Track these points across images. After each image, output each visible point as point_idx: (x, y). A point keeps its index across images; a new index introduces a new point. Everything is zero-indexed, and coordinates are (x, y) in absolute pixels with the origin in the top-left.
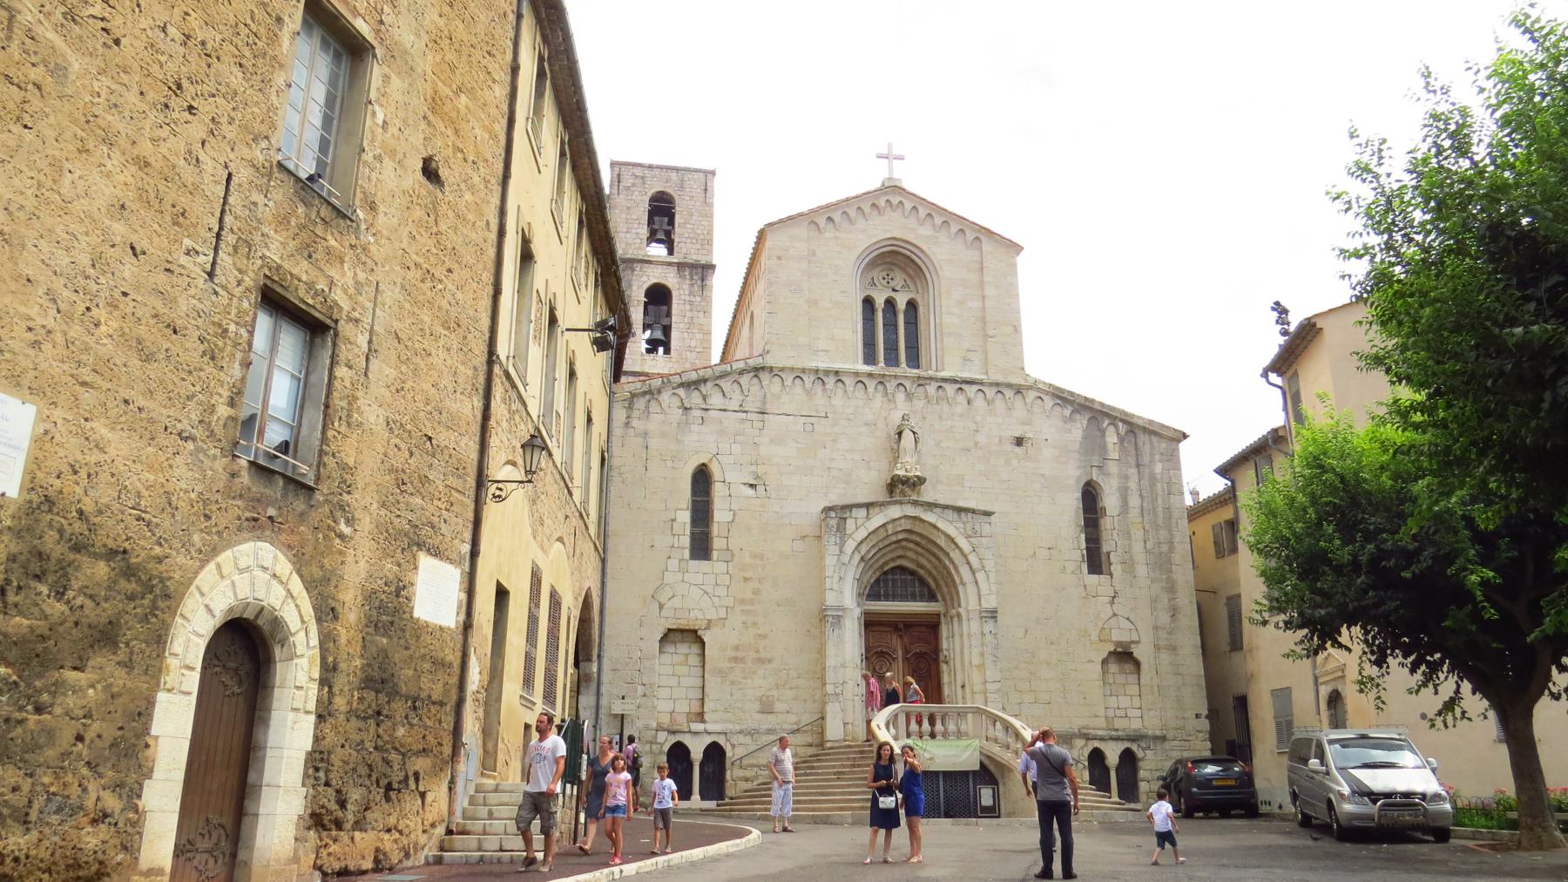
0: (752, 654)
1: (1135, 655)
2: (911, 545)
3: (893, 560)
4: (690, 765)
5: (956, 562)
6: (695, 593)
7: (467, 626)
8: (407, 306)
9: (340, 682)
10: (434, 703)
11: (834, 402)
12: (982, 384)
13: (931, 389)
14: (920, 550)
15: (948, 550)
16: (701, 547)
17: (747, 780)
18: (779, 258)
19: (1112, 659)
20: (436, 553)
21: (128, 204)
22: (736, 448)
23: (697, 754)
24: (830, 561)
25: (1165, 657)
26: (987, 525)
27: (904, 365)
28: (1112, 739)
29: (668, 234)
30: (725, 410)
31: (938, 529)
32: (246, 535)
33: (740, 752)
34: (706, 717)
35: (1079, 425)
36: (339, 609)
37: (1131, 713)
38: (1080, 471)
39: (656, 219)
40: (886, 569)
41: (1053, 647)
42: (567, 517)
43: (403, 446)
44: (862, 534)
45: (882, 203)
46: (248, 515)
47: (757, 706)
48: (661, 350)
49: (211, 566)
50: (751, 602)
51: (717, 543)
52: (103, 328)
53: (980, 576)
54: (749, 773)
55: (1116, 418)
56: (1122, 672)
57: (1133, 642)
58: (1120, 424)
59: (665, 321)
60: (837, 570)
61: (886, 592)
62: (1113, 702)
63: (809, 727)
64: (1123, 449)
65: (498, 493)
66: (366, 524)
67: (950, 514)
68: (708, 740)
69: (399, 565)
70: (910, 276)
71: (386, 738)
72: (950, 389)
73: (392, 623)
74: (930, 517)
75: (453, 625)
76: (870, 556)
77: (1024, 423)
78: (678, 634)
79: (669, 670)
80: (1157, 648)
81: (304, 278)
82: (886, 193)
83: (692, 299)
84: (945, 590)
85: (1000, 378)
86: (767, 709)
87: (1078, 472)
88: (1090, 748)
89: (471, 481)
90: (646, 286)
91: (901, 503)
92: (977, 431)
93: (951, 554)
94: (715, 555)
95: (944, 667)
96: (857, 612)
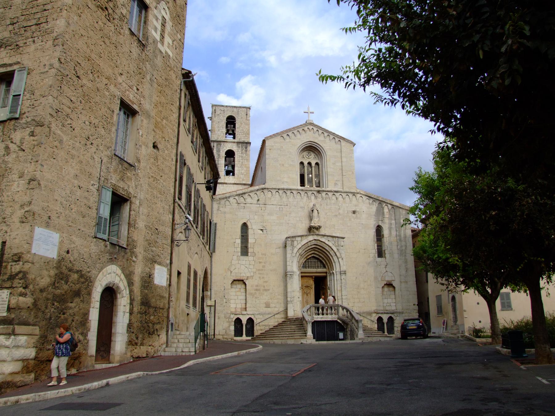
0: (262, 288)
1: (393, 285)
2: (317, 249)
3: (311, 254)
4: (242, 325)
5: (332, 255)
6: (243, 267)
7: (170, 285)
8: (150, 190)
9: (135, 304)
10: (161, 309)
11: (290, 200)
12: (342, 192)
13: (324, 194)
14: (320, 251)
16: (245, 251)
17: (261, 330)
18: (270, 149)
19: (386, 286)
20: (160, 264)
21: (78, 174)
22: (256, 217)
23: (244, 322)
24: (289, 255)
25: (403, 285)
26: (343, 242)
27: (314, 186)
28: (385, 313)
29: (233, 131)
30: (252, 204)
31: (326, 244)
32: (109, 263)
33: (259, 321)
34: (247, 309)
35: (375, 206)
36: (134, 283)
37: (392, 304)
38: (375, 222)
39: (229, 125)
40: (308, 257)
42: (198, 245)
43: (150, 233)
44: (300, 246)
45: (306, 128)
46: (110, 258)
47: (265, 305)
48: (231, 174)
49: (101, 273)
50: (262, 270)
51: (250, 250)
52: (73, 210)
53: (340, 260)
54: (262, 328)
55: (387, 203)
56: (389, 291)
57: (394, 280)
58: (389, 205)
59: (233, 163)
61: (308, 265)
62: (386, 301)
64: (390, 214)
65: (177, 244)
66: (140, 257)
67: (330, 239)
68: (248, 317)
69: (150, 268)
70: (317, 155)
71: (148, 319)
72: (330, 194)
73: (148, 286)
74: (323, 239)
75: (165, 285)
77: (356, 206)
78: (237, 282)
79: (234, 294)
80: (401, 282)
81: (122, 187)
82: (307, 125)
83: (242, 155)
84: (329, 265)
85: (347, 190)
86: (268, 306)
87: (375, 222)
88: (378, 317)
89: (169, 241)
90: (225, 151)
91: (313, 235)
92: (339, 209)
93: (331, 252)
94: (249, 254)
95: (329, 291)
96: (298, 273)
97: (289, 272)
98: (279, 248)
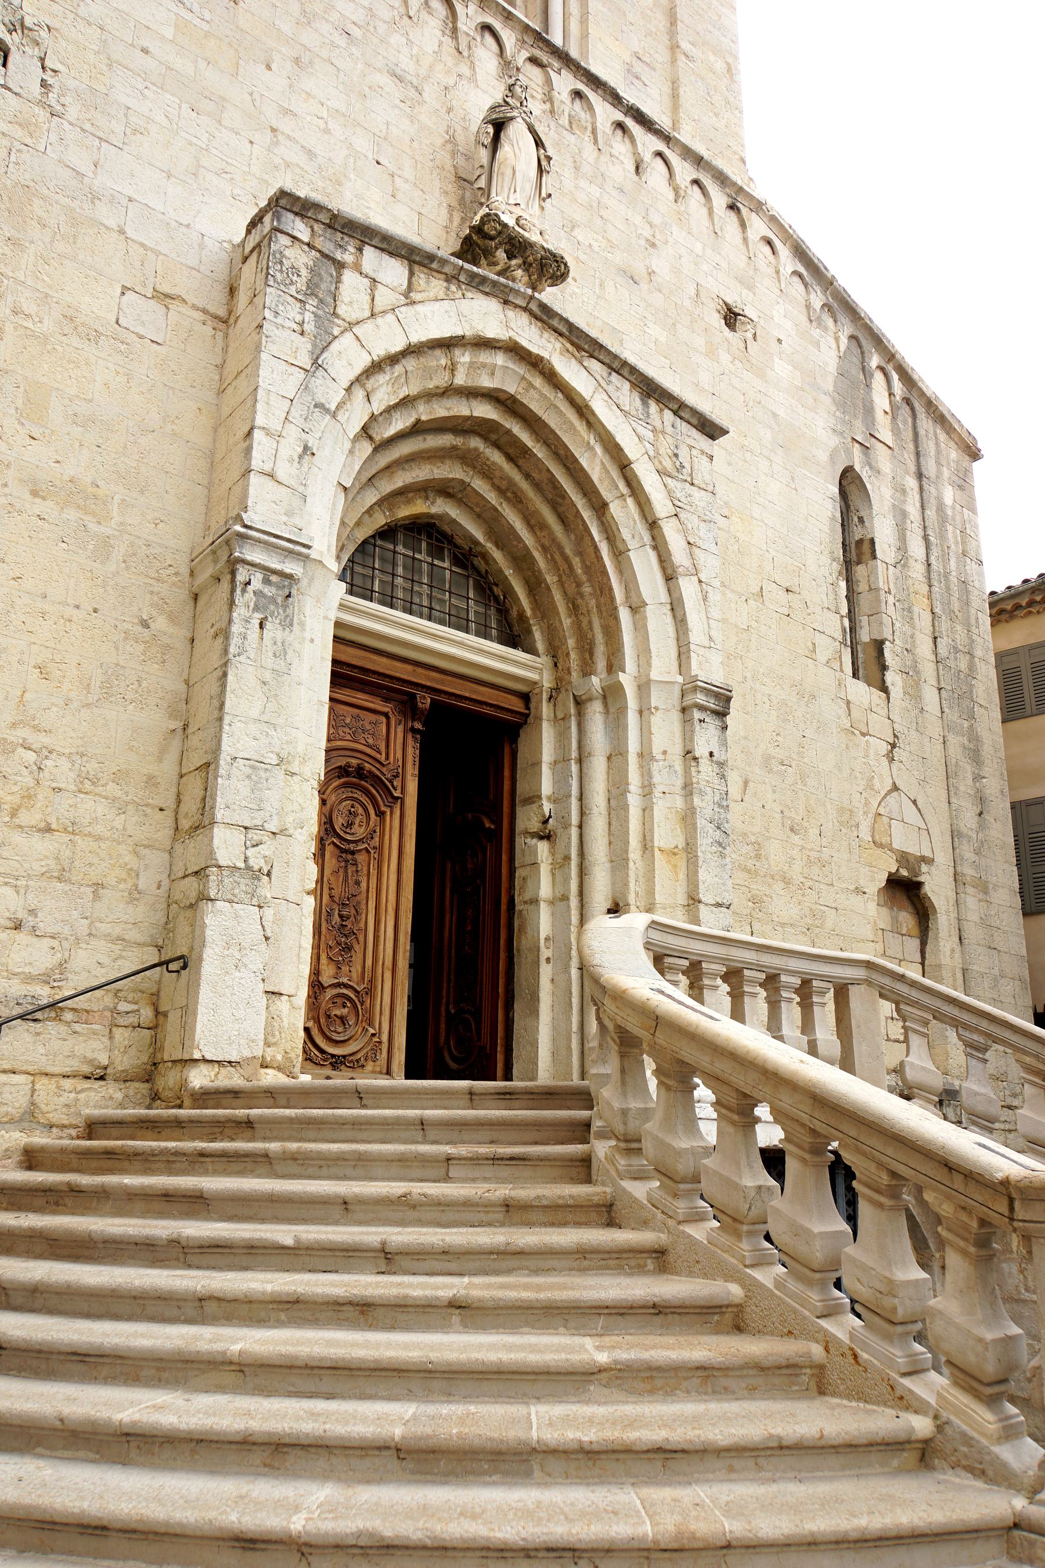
3: (423, 489)
5: (625, 534)
15: (606, 494)
40: (404, 512)
41: (796, 839)
57: (923, 859)
60: (295, 414)
63: (101, 1000)
64: (896, 431)
76: (391, 431)
92: (653, 245)
93: (615, 509)
97: (272, 542)
98: (164, 298)
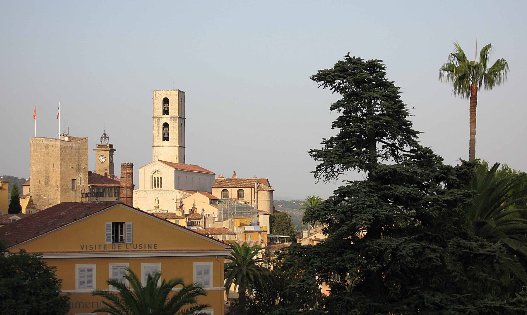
83: (173, 126)
